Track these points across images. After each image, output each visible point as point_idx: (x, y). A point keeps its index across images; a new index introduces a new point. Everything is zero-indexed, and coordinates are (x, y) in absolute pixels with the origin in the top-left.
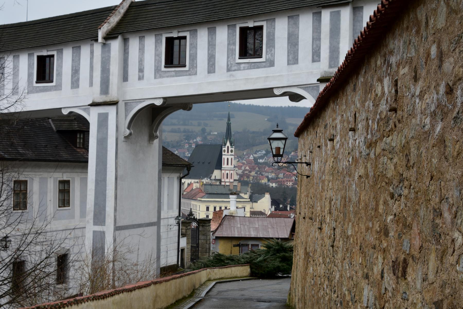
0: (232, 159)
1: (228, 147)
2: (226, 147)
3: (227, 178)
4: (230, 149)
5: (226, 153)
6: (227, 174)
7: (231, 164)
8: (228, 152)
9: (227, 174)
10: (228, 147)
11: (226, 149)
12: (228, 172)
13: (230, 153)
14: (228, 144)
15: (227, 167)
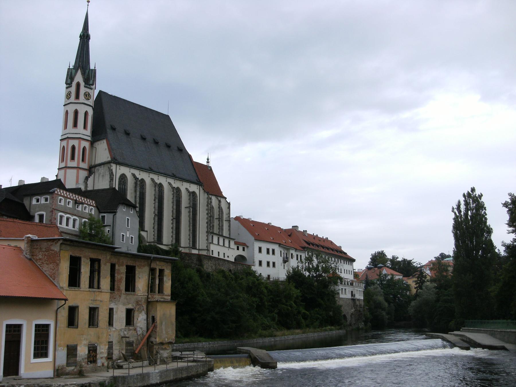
0: (86, 113)
1: (78, 85)
2: (74, 84)
3: (73, 158)
4: (83, 90)
5: (73, 99)
6: (73, 148)
7: (85, 127)
8: (77, 97)
9: (73, 148)
10: (78, 85)
11: (73, 89)
12: (76, 143)
13: (82, 98)
14: (79, 78)
15: (75, 131)
